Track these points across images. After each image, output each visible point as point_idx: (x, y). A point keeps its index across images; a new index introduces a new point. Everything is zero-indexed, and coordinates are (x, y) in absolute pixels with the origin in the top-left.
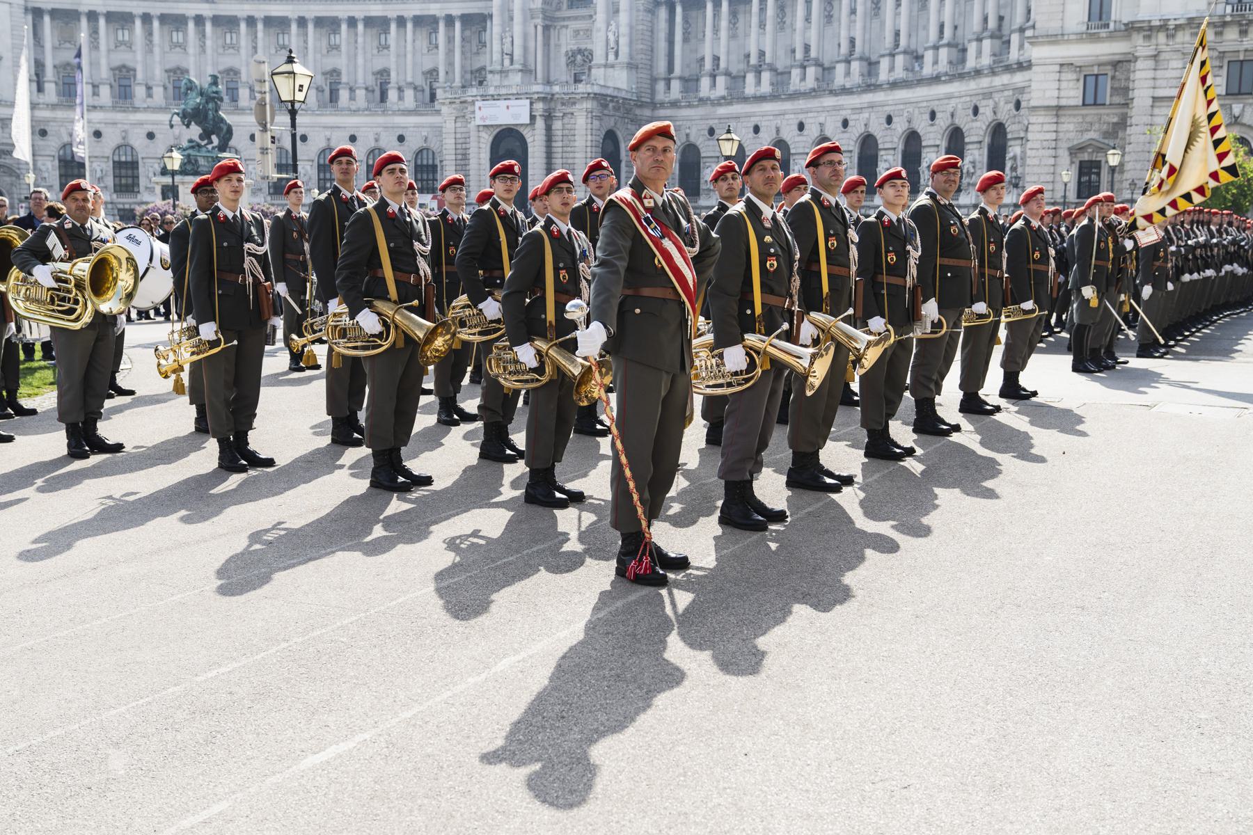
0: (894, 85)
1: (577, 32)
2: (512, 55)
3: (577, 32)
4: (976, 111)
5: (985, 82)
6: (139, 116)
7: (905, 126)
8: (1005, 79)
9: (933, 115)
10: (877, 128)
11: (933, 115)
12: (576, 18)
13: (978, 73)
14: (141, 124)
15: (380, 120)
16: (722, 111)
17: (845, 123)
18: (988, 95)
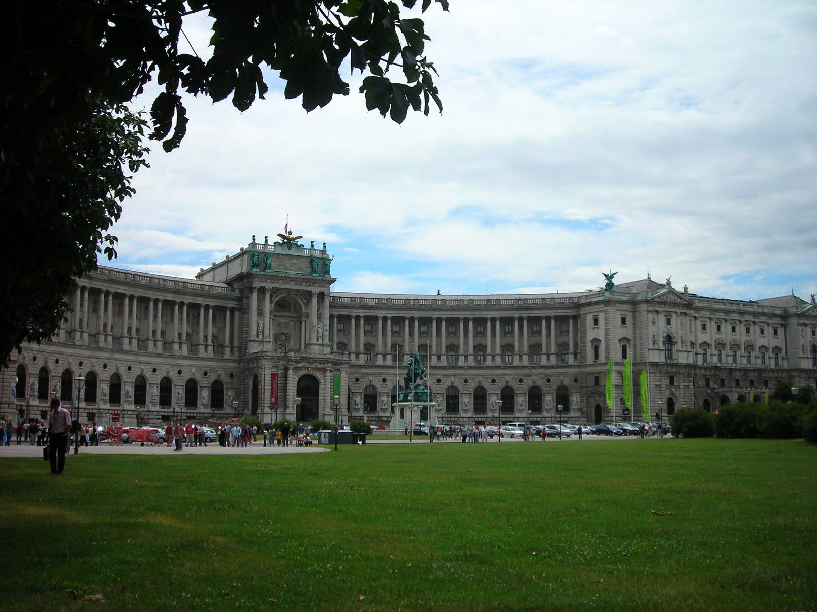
0: (471, 368)
1: (280, 323)
2: (263, 332)
3: (280, 323)
4: (521, 381)
5: (527, 371)
6: (53, 348)
7: (477, 384)
8: (540, 371)
9: (494, 381)
10: (458, 383)
11: (494, 381)
12: (280, 316)
13: (524, 367)
14: (54, 353)
15: (170, 361)
16: (364, 371)
17: (439, 381)
18: (529, 376)
